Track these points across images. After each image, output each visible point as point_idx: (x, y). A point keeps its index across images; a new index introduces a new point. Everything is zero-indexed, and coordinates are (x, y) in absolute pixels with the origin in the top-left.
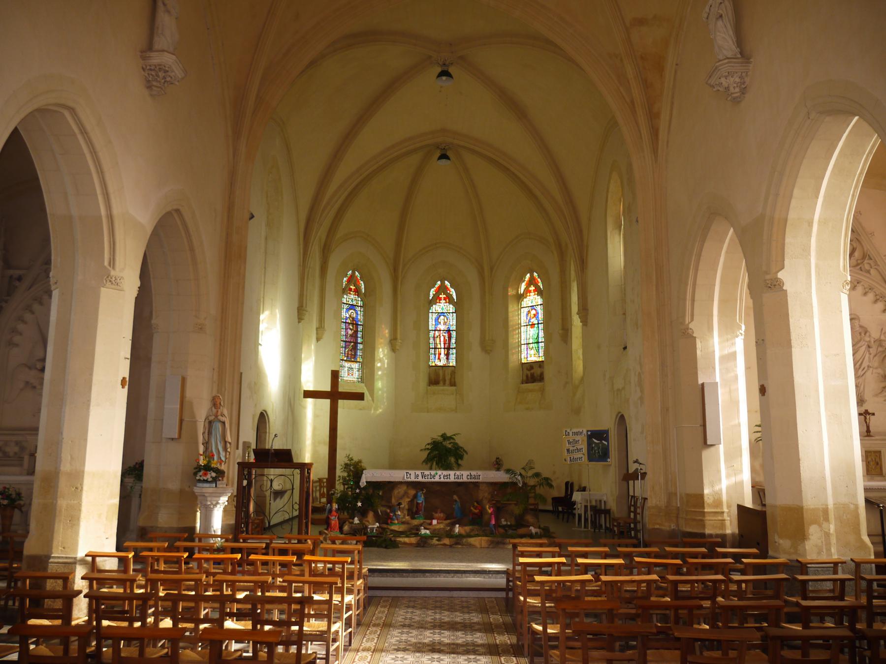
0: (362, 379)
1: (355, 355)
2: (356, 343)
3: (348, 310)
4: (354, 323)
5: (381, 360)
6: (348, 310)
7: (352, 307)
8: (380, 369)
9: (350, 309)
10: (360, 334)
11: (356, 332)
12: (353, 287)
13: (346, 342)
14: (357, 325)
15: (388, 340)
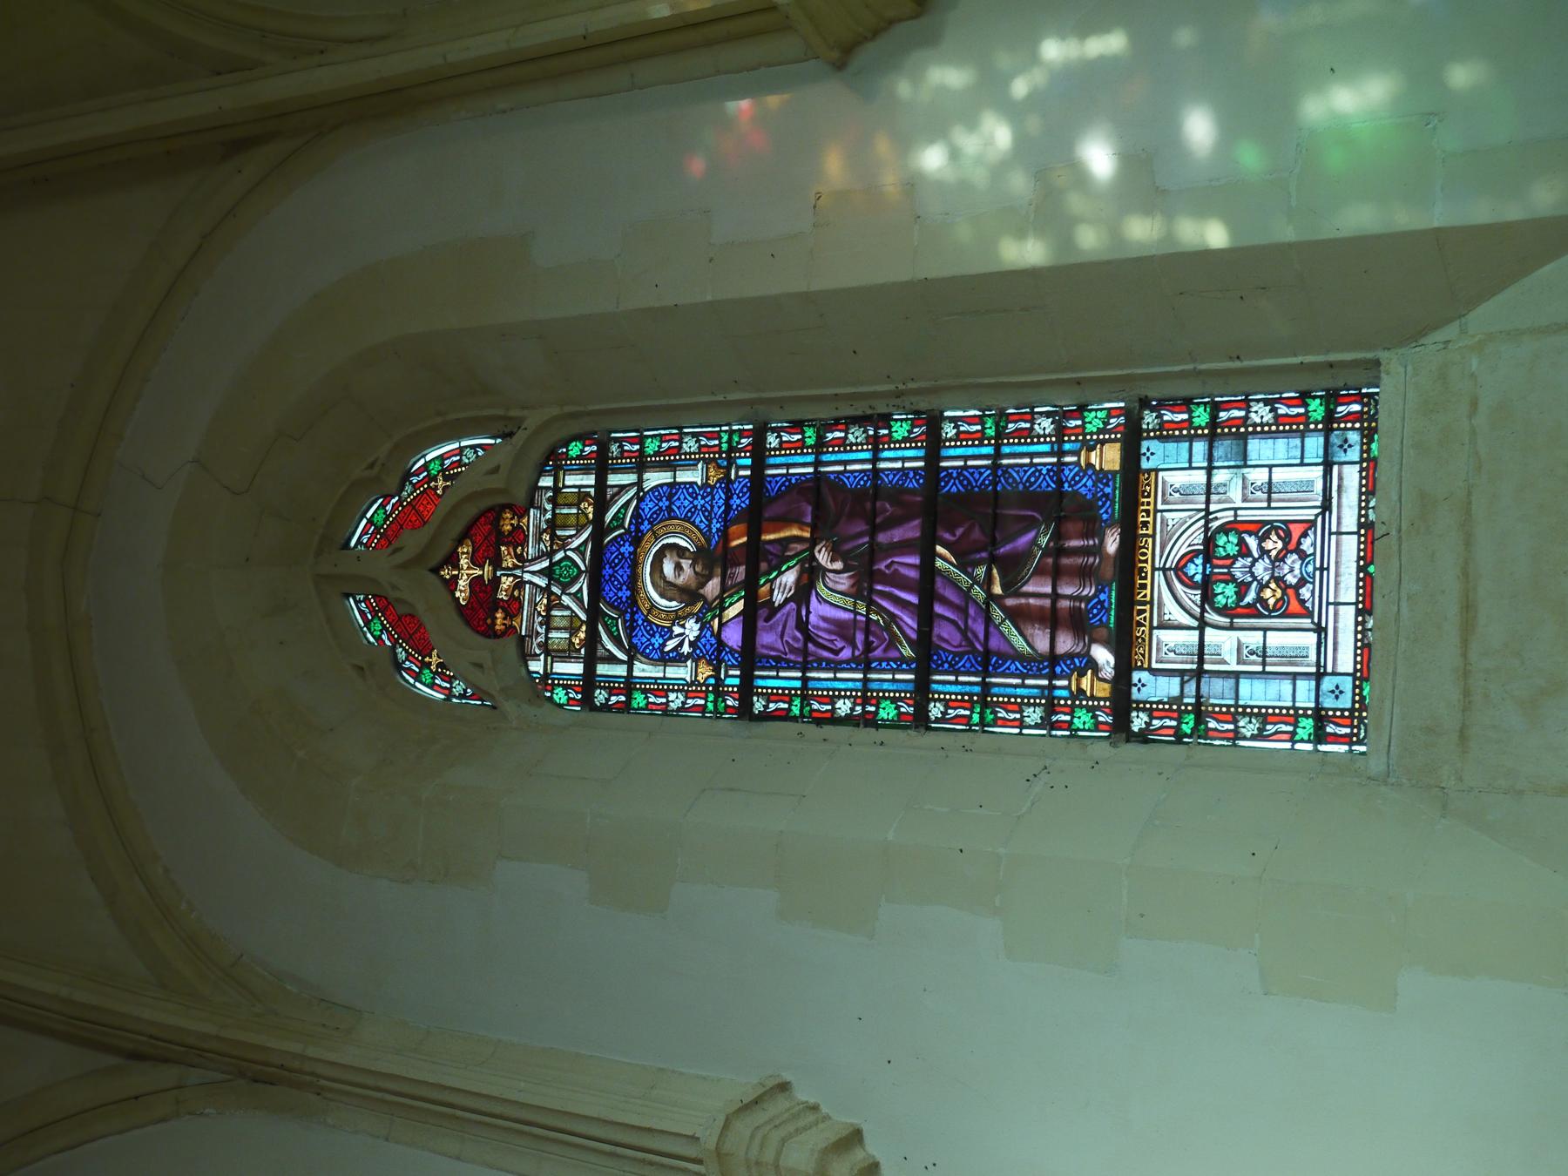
0: (1336, 399)
1: (1062, 506)
2: (938, 504)
3: (642, 636)
4: (751, 529)
5: (1047, 155)
6: (642, 636)
7: (612, 575)
8: (1151, 174)
9: (631, 605)
10: (851, 459)
11: (824, 502)
12: (466, 572)
13: (927, 660)
14: (763, 501)
15: (827, 97)
